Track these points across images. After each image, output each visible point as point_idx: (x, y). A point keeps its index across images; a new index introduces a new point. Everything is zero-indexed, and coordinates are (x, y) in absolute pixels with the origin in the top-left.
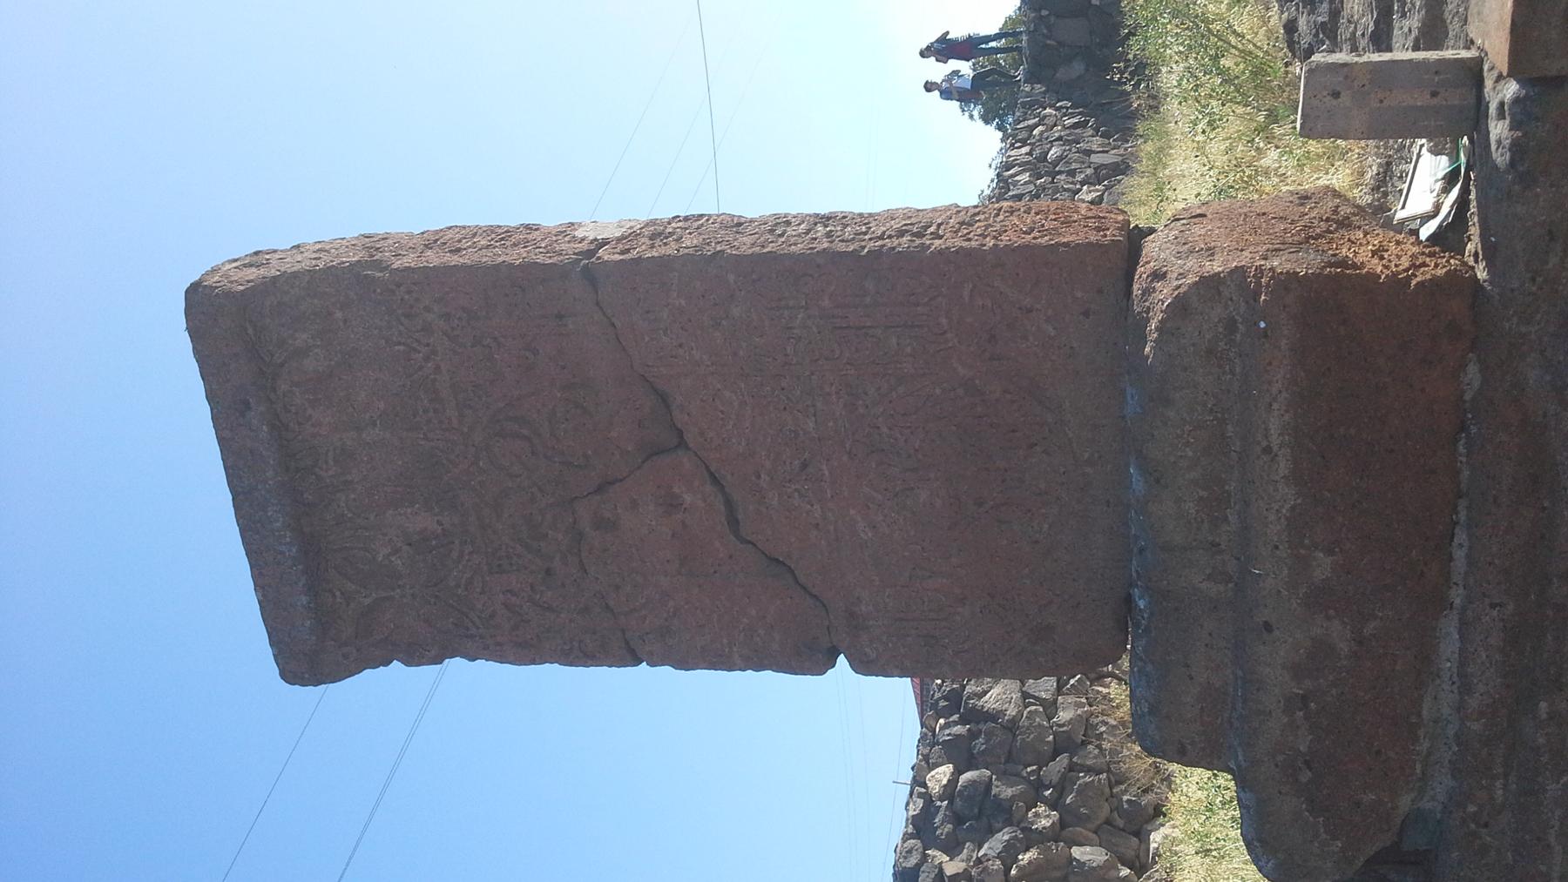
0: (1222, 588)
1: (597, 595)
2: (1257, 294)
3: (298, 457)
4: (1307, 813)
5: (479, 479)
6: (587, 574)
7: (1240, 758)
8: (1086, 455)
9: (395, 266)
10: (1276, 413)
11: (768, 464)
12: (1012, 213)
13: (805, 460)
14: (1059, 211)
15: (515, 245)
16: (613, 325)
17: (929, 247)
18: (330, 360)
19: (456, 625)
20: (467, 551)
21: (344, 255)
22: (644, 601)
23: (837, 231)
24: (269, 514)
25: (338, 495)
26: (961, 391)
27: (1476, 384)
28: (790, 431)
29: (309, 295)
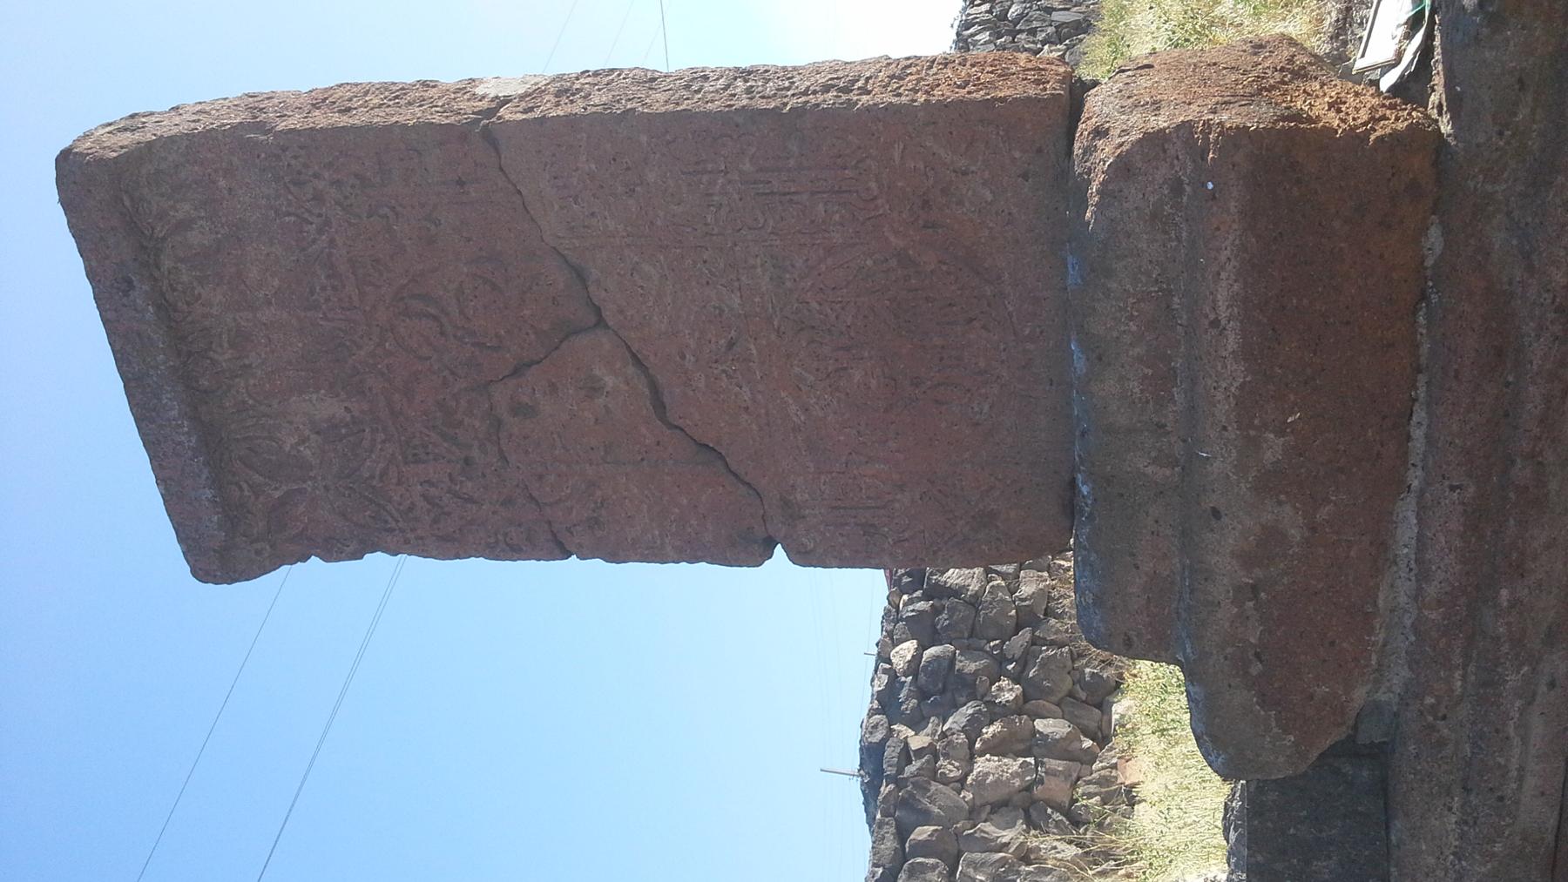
0: (1168, 473)
1: (521, 485)
2: (1205, 152)
3: (190, 339)
5: (386, 362)
6: (508, 462)
7: (1189, 650)
9: (279, 128)
10: (1224, 284)
12: (946, 65)
13: (732, 338)
14: (996, 62)
15: (410, 104)
16: (519, 192)
17: (856, 103)
18: (217, 233)
19: (373, 517)
20: (379, 440)
21: (225, 117)
22: (569, 491)
23: (758, 86)
25: (237, 380)
26: (893, 263)
27: (1438, 249)
28: (715, 308)
29: (188, 161)
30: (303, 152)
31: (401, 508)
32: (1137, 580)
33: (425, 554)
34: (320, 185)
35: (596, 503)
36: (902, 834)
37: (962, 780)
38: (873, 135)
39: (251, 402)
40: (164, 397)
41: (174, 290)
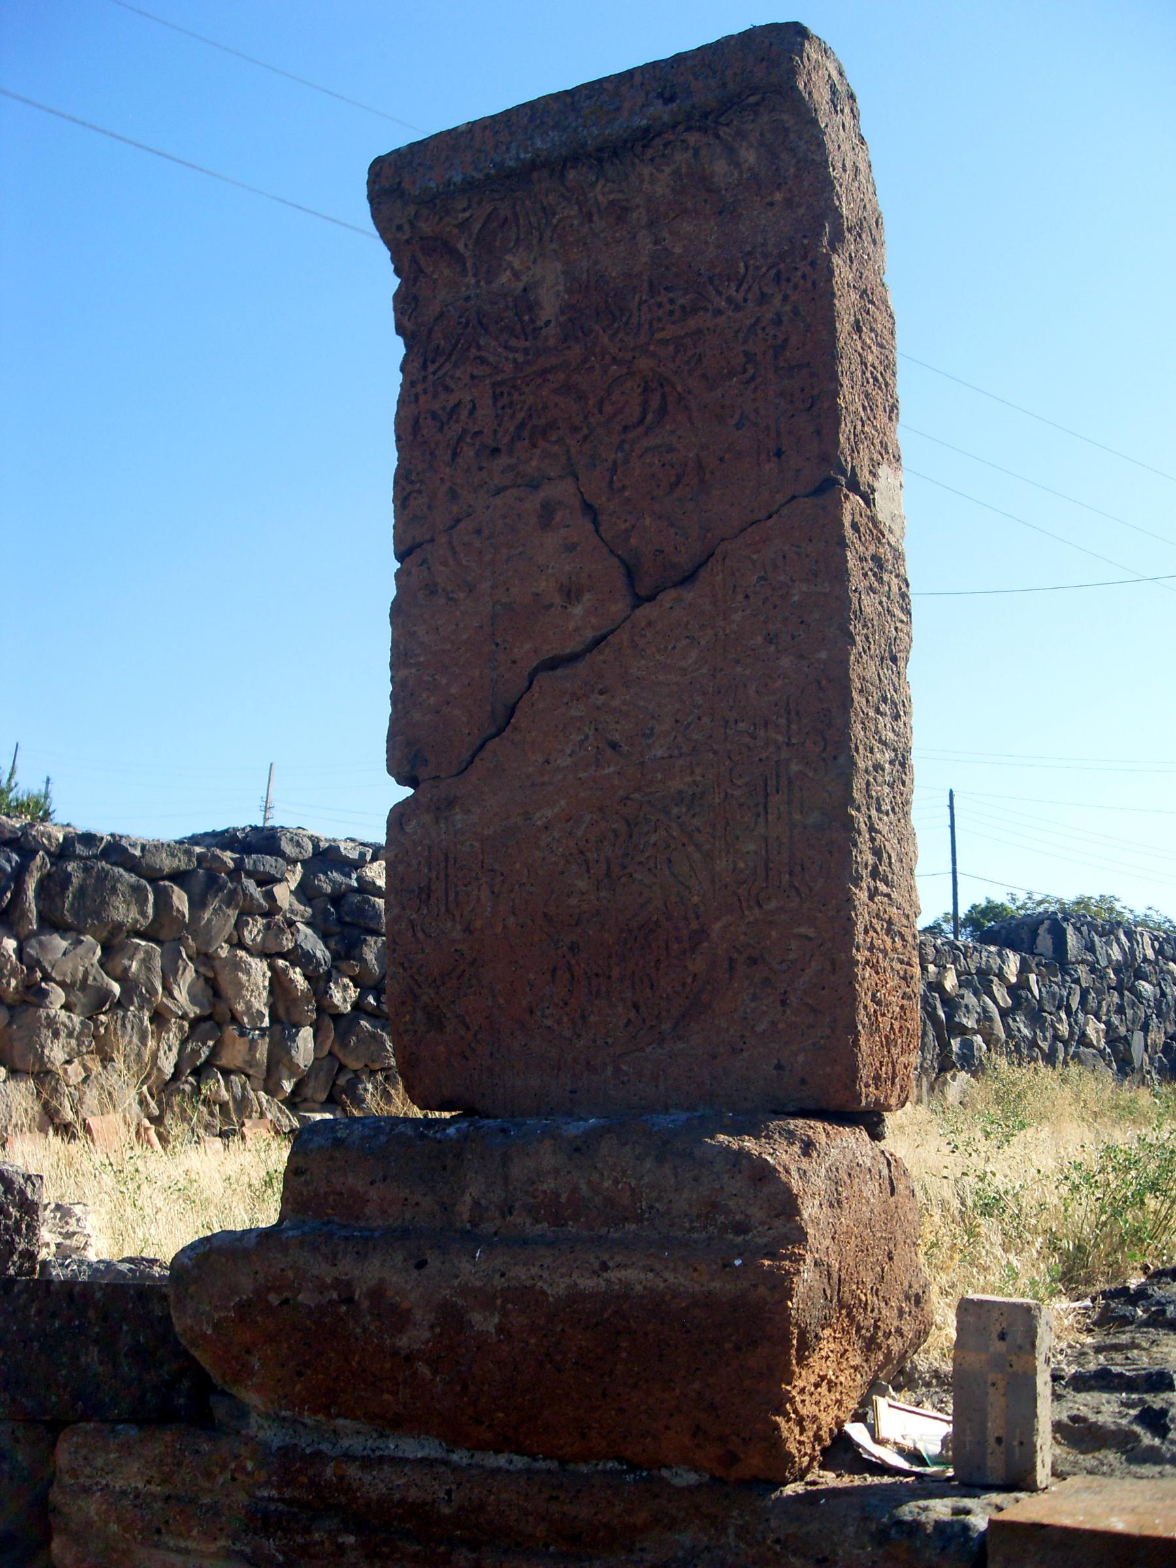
0: (466, 1216)
1: (470, 510)
2: (772, 1256)
4: (238, 1299)
5: (597, 366)
6: (494, 495)
7: (291, 1233)
8: (624, 1068)
9: (835, 259)
10: (642, 1276)
11: (616, 703)
12: (904, 978)
14: (905, 1033)
15: (867, 395)
16: (770, 517)
17: (856, 886)
18: (726, 190)
19: (438, 347)
21: (850, 198)
22: (464, 562)
23: (883, 776)
24: (550, 133)
25: (576, 208)
26: (695, 925)
27: (677, 1482)
28: (652, 729)
29: (798, 162)
30: (809, 285)
31: (447, 379)
32: (360, 1183)
33: (402, 402)
34: (777, 301)
35: (452, 592)
36: (178, 877)
37: (241, 945)
38: (824, 905)
39: (555, 221)
40: (555, 133)
41: (666, 145)
